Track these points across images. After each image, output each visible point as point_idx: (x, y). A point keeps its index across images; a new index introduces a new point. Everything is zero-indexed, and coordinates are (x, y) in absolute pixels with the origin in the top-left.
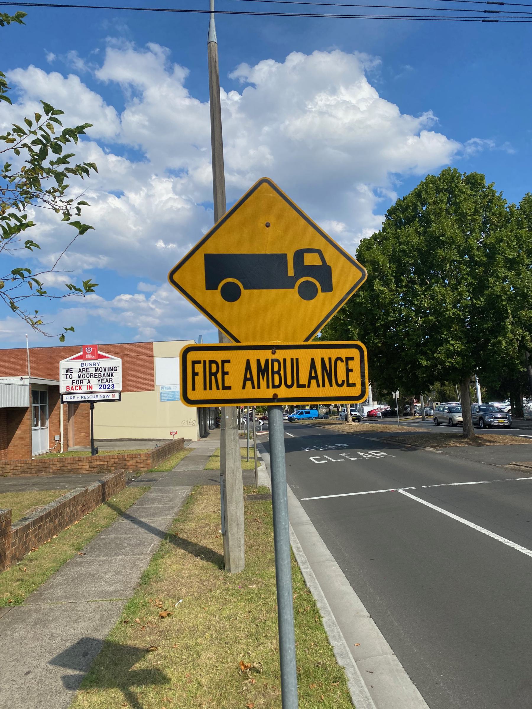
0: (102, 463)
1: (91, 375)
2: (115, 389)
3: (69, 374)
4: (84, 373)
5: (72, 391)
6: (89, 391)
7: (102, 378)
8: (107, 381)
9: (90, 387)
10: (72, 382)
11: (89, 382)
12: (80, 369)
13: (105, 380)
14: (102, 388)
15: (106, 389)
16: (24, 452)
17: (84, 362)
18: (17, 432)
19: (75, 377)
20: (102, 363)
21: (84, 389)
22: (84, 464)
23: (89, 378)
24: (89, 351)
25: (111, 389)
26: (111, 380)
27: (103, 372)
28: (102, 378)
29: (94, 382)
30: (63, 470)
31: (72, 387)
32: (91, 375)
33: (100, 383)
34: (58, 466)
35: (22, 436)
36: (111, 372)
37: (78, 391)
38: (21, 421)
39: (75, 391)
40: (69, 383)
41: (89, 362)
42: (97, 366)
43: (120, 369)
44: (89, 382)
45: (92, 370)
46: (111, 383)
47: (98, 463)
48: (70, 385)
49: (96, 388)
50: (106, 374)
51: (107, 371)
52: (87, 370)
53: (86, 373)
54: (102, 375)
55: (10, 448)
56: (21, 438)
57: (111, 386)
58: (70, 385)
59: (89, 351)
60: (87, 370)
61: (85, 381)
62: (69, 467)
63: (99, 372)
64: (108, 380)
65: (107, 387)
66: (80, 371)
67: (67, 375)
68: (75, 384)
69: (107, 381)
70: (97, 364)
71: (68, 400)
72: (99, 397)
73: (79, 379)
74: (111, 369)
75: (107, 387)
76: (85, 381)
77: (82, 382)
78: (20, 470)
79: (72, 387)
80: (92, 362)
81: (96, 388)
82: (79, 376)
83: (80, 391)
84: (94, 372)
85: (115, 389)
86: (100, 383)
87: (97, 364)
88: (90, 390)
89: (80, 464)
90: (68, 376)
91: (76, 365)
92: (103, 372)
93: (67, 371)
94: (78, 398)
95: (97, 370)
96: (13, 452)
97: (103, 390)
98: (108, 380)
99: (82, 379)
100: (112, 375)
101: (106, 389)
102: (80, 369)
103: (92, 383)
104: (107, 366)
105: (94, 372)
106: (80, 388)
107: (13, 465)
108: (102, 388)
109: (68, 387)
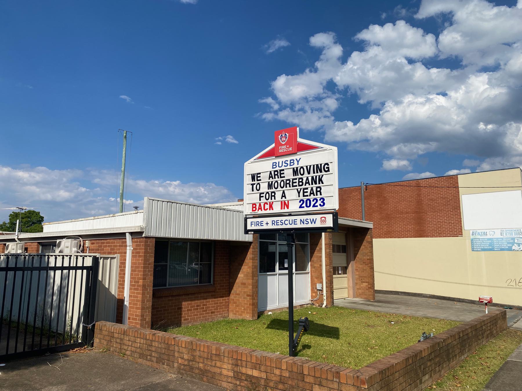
0: (256, 373)
1: (287, 183)
2: (326, 207)
3: (256, 182)
4: (277, 179)
5: (260, 212)
6: (283, 211)
7: (304, 187)
8: (312, 193)
9: (285, 205)
10: (260, 197)
11: (284, 196)
12: (271, 173)
13: (309, 190)
14: (304, 205)
15: (311, 208)
16: (247, 304)
17: (277, 161)
18: (239, 276)
19: (264, 188)
20: (306, 159)
21: (277, 208)
22: (225, 366)
23: (285, 188)
24: (284, 139)
25: (319, 208)
26: (319, 190)
27: (306, 174)
28: (304, 187)
29: (292, 194)
30: (192, 368)
31: (260, 205)
32: (287, 183)
33: (301, 197)
34: (186, 357)
35: (244, 281)
36: (319, 174)
37: (268, 212)
38: (243, 261)
39: (264, 212)
40: (255, 198)
41: (284, 159)
42: (295, 166)
43: (334, 168)
44: (284, 196)
45: (288, 174)
46: (319, 197)
47: (250, 372)
48: (257, 201)
49: (294, 207)
50: (310, 179)
51: (312, 174)
52: (280, 173)
53: (279, 180)
54: (304, 181)
55: (232, 296)
56: (243, 284)
57: (319, 202)
58: (257, 201)
59: (284, 139)
60: (280, 173)
61: (279, 195)
62: (201, 365)
63: (300, 176)
64: (314, 189)
65: (312, 203)
66: (270, 177)
67: (253, 185)
68: (263, 200)
69: (312, 193)
70: (296, 162)
71: (254, 227)
72: (298, 222)
73: (270, 191)
74: (318, 168)
75: (312, 203)
76: (279, 195)
77: (273, 195)
78: (138, 350)
79: (260, 205)
80: (289, 158)
81: (294, 207)
82: (270, 186)
83: (271, 211)
84: (291, 177)
85: (326, 207)
86: (301, 197)
87: (296, 162)
88: (286, 210)
89: (218, 364)
90: (255, 186)
91: (265, 167)
92: (306, 174)
93: (253, 178)
94: (268, 224)
95: (295, 172)
96: (235, 303)
97: (306, 209)
98: (314, 189)
99: (274, 190)
100: (320, 180)
101: (311, 208)
102: (271, 173)
103: (288, 198)
104: (312, 164)
105: (291, 177)
106: (271, 207)
107: (132, 339)
108: (304, 205)
109: (254, 205)
